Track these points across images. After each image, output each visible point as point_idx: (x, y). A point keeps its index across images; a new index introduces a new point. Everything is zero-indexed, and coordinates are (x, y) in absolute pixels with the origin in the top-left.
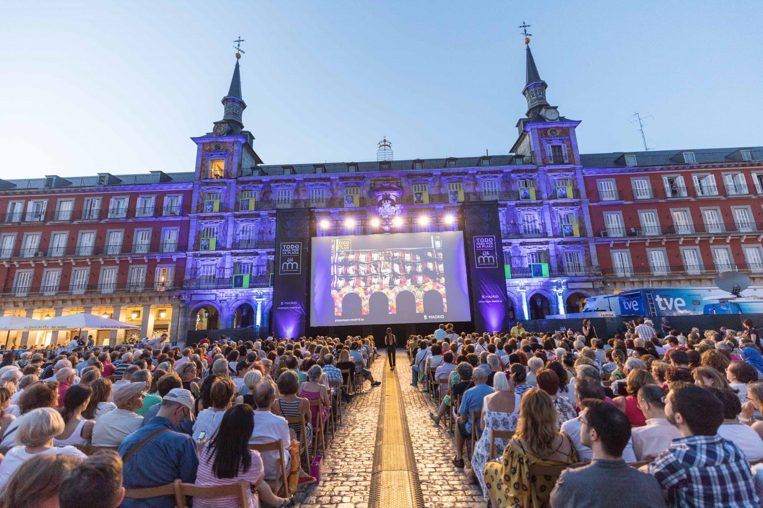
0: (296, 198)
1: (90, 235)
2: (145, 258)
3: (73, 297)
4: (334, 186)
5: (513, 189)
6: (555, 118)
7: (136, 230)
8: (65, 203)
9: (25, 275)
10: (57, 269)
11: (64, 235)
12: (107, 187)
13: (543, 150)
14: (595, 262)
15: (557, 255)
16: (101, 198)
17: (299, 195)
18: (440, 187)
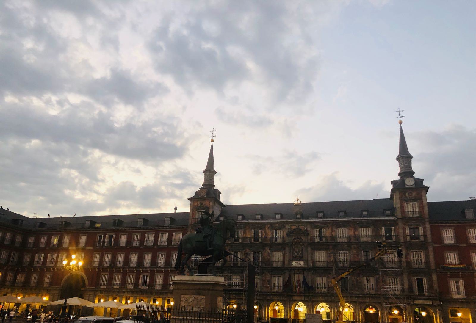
0: (244, 236)
1: (135, 255)
2: (163, 270)
3: (129, 290)
4: (267, 229)
5: (380, 233)
6: (412, 184)
7: (158, 252)
8: (123, 235)
9: (105, 276)
10: (120, 274)
11: (123, 254)
12: (144, 228)
13: (402, 207)
14: (436, 286)
15: (409, 281)
16: (140, 233)
17: (246, 233)
18: (332, 231)
